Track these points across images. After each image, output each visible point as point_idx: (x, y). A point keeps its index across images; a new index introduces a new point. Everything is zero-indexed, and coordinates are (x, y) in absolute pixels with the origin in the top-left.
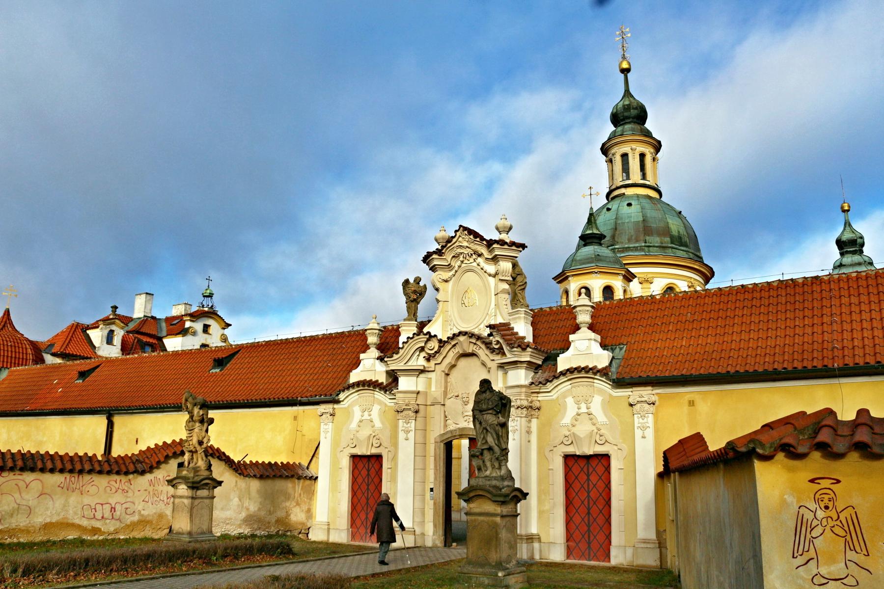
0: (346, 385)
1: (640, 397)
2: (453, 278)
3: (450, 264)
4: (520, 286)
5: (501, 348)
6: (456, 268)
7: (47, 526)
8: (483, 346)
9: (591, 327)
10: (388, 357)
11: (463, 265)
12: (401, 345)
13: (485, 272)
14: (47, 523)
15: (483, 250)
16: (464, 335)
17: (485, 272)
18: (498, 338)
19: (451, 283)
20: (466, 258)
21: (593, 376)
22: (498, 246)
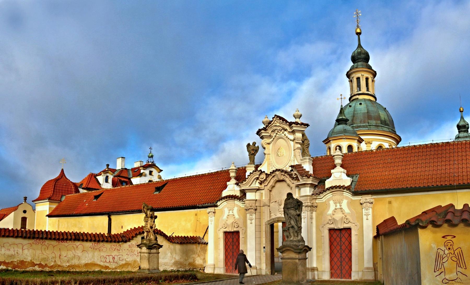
0: (220, 198)
1: (365, 200)
2: (272, 142)
3: (270, 135)
4: (306, 145)
5: (297, 177)
6: (274, 137)
7: (86, 265)
8: (288, 176)
9: (342, 166)
10: (240, 183)
11: (277, 135)
12: (247, 177)
13: (289, 139)
15: (287, 128)
16: (279, 171)
17: (289, 139)
18: (295, 172)
19: (271, 145)
20: (278, 132)
21: (343, 190)
22: (295, 125)
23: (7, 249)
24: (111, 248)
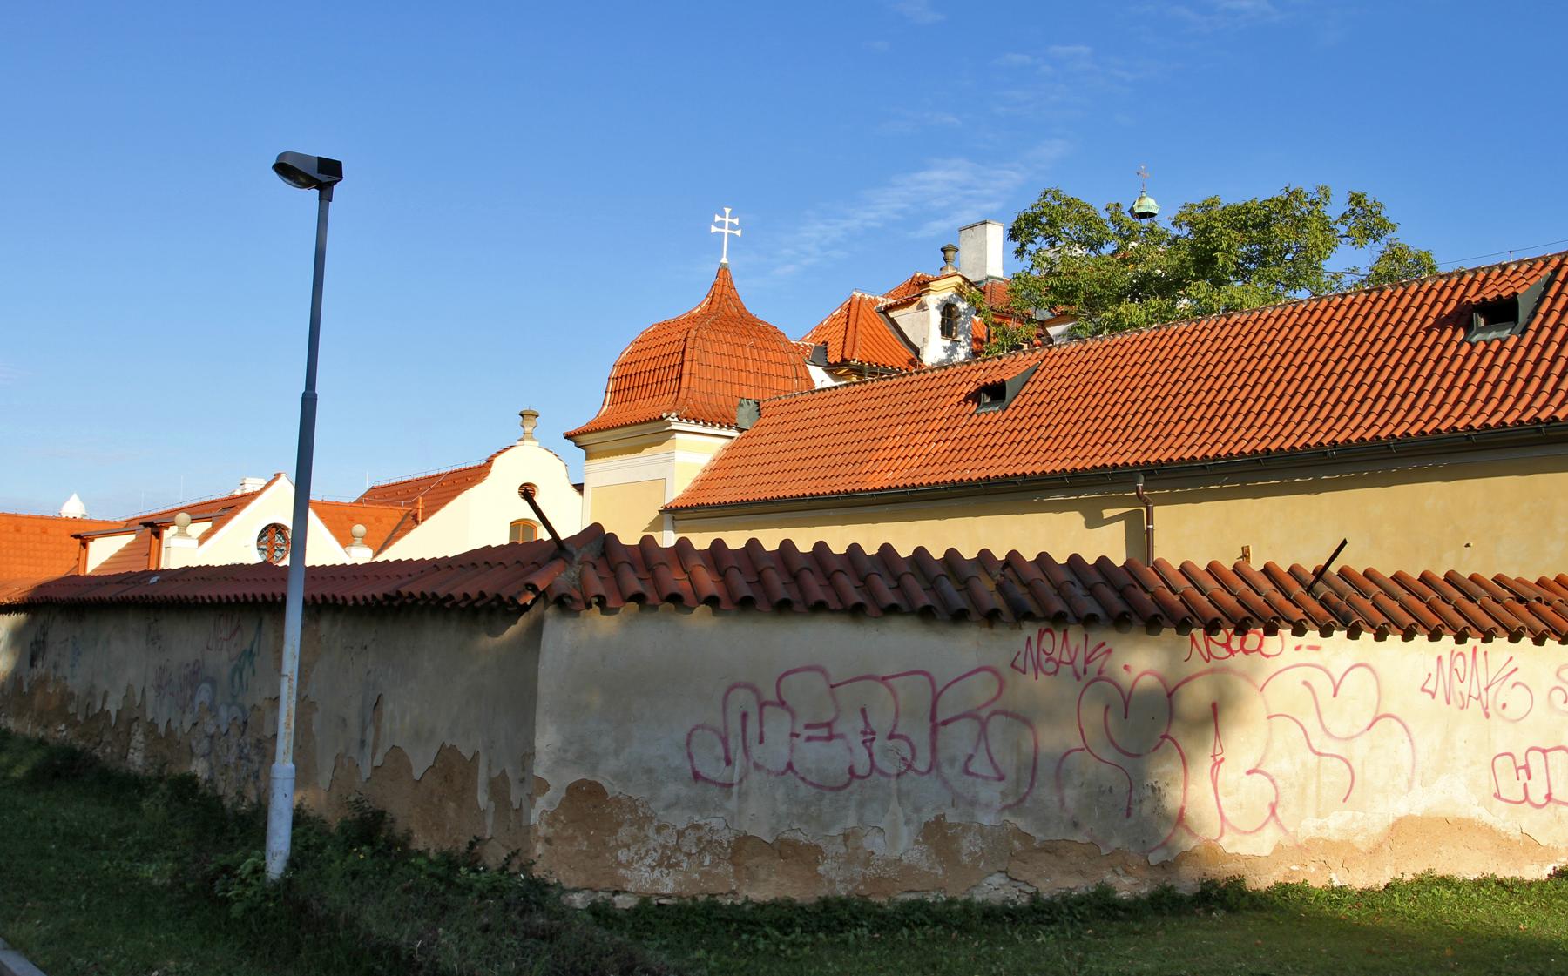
7: (1400, 829)
14: (1400, 820)
23: (808, 726)
24: (1559, 691)
